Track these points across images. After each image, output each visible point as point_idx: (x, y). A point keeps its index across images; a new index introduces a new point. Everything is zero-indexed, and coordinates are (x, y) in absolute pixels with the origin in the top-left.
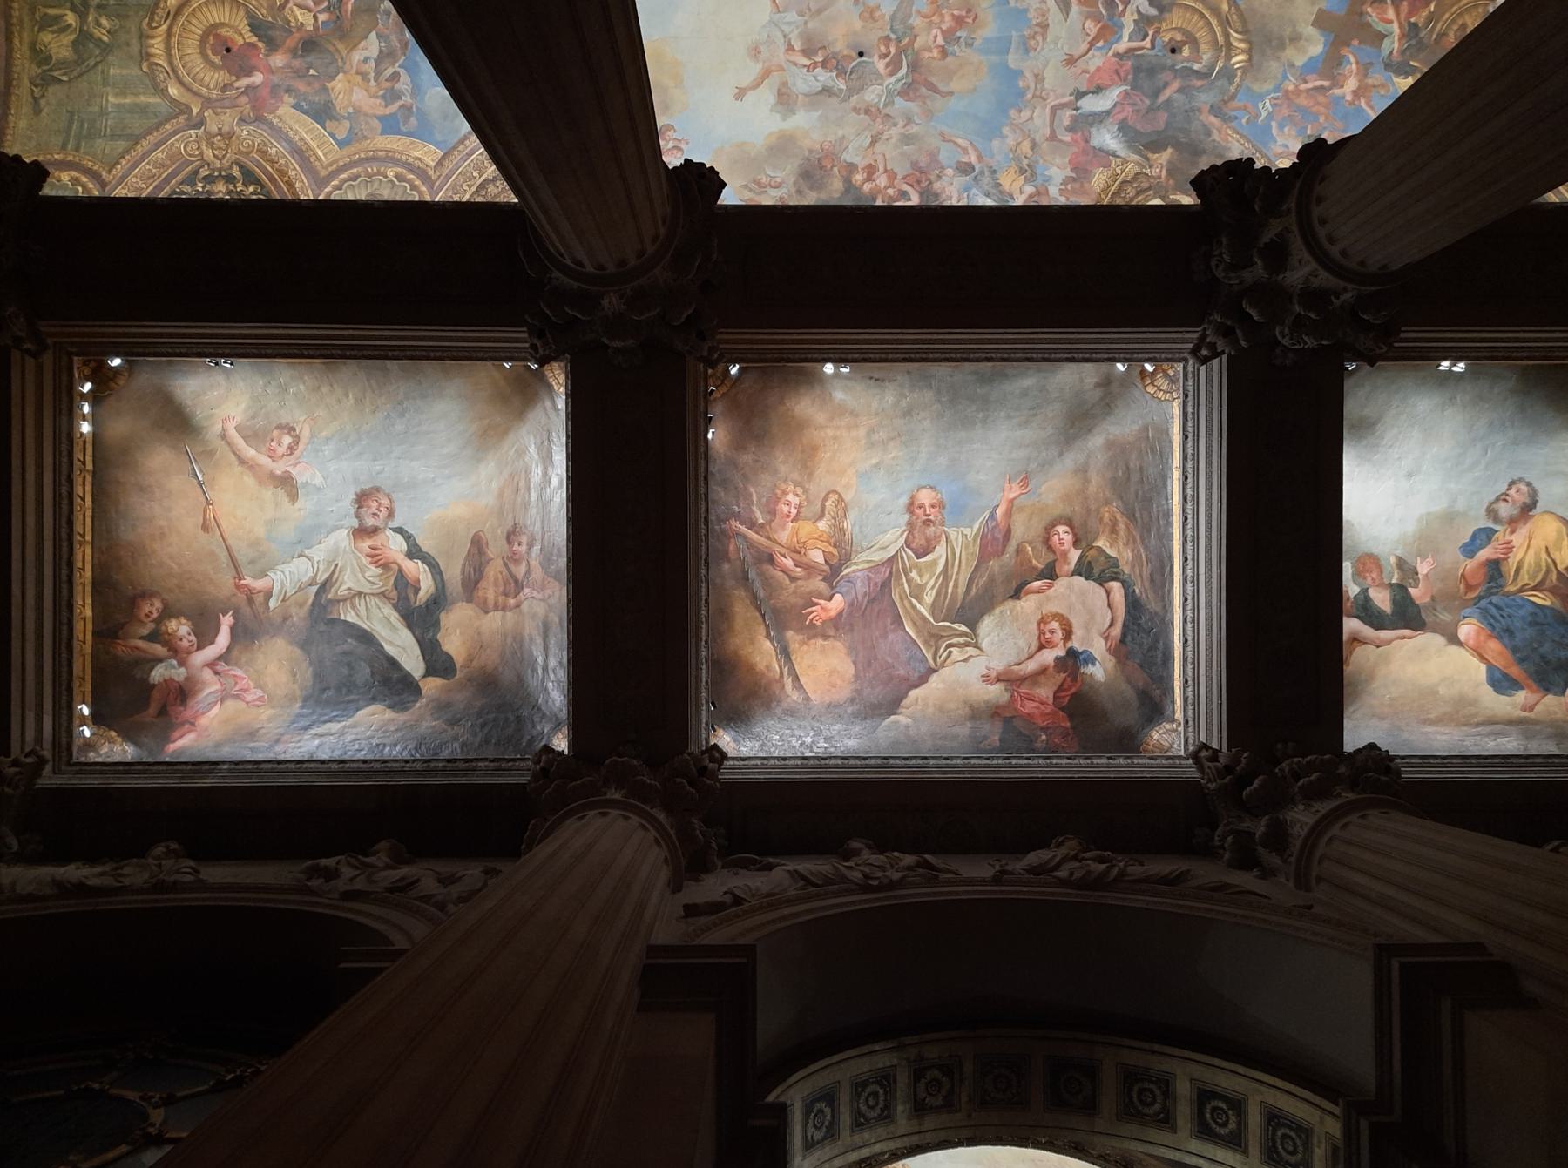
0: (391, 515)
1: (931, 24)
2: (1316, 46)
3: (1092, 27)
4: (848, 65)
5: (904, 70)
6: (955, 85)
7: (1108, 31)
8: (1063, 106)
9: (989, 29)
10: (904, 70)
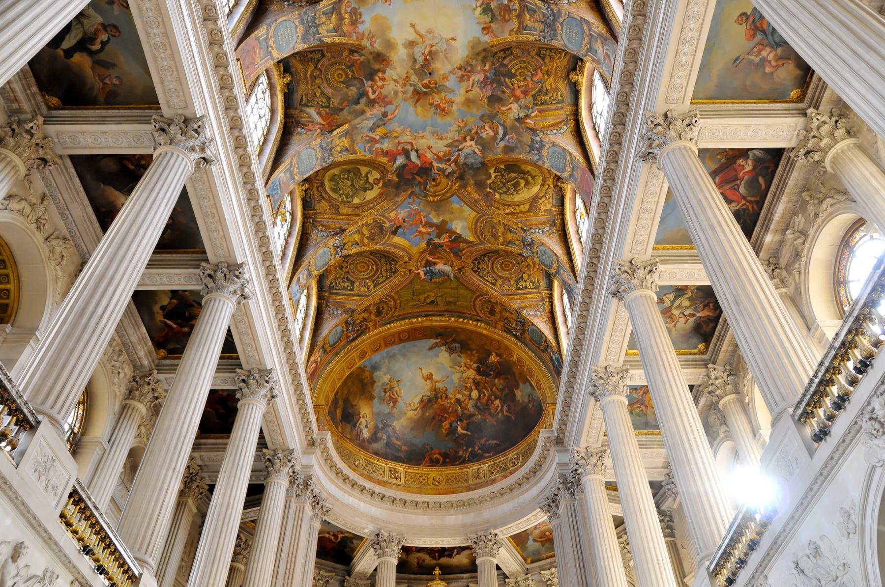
0: (114, 36)
1: (442, 99)
2: (436, 220)
3: (441, 154)
4: (425, 68)
5: (424, 90)
6: (419, 109)
7: (439, 159)
8: (412, 145)
9: (439, 120)
10: (424, 90)
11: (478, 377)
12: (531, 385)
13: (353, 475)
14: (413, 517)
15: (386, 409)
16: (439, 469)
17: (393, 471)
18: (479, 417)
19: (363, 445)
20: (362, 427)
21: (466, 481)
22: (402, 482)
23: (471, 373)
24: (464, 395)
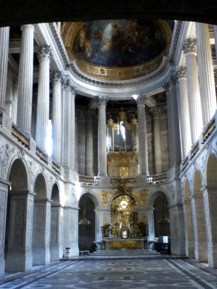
11: (138, 26)
12: (162, 32)
13: (85, 76)
14: (111, 89)
15: (97, 42)
16: (121, 68)
17: (102, 71)
18: (138, 44)
19: (89, 60)
20: (87, 51)
21: (133, 73)
22: (106, 75)
23: (135, 24)
24: (132, 34)
